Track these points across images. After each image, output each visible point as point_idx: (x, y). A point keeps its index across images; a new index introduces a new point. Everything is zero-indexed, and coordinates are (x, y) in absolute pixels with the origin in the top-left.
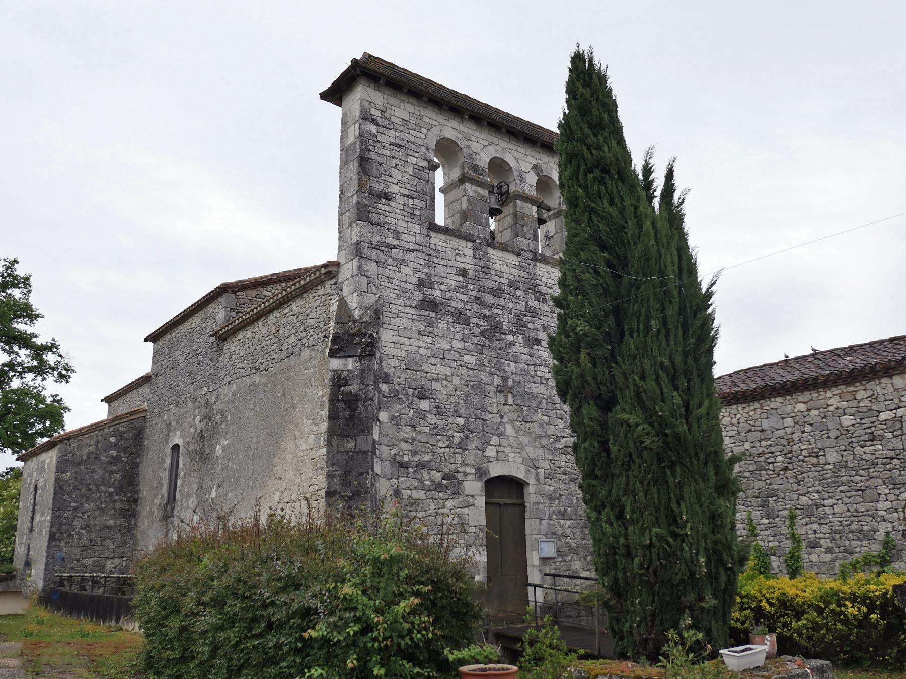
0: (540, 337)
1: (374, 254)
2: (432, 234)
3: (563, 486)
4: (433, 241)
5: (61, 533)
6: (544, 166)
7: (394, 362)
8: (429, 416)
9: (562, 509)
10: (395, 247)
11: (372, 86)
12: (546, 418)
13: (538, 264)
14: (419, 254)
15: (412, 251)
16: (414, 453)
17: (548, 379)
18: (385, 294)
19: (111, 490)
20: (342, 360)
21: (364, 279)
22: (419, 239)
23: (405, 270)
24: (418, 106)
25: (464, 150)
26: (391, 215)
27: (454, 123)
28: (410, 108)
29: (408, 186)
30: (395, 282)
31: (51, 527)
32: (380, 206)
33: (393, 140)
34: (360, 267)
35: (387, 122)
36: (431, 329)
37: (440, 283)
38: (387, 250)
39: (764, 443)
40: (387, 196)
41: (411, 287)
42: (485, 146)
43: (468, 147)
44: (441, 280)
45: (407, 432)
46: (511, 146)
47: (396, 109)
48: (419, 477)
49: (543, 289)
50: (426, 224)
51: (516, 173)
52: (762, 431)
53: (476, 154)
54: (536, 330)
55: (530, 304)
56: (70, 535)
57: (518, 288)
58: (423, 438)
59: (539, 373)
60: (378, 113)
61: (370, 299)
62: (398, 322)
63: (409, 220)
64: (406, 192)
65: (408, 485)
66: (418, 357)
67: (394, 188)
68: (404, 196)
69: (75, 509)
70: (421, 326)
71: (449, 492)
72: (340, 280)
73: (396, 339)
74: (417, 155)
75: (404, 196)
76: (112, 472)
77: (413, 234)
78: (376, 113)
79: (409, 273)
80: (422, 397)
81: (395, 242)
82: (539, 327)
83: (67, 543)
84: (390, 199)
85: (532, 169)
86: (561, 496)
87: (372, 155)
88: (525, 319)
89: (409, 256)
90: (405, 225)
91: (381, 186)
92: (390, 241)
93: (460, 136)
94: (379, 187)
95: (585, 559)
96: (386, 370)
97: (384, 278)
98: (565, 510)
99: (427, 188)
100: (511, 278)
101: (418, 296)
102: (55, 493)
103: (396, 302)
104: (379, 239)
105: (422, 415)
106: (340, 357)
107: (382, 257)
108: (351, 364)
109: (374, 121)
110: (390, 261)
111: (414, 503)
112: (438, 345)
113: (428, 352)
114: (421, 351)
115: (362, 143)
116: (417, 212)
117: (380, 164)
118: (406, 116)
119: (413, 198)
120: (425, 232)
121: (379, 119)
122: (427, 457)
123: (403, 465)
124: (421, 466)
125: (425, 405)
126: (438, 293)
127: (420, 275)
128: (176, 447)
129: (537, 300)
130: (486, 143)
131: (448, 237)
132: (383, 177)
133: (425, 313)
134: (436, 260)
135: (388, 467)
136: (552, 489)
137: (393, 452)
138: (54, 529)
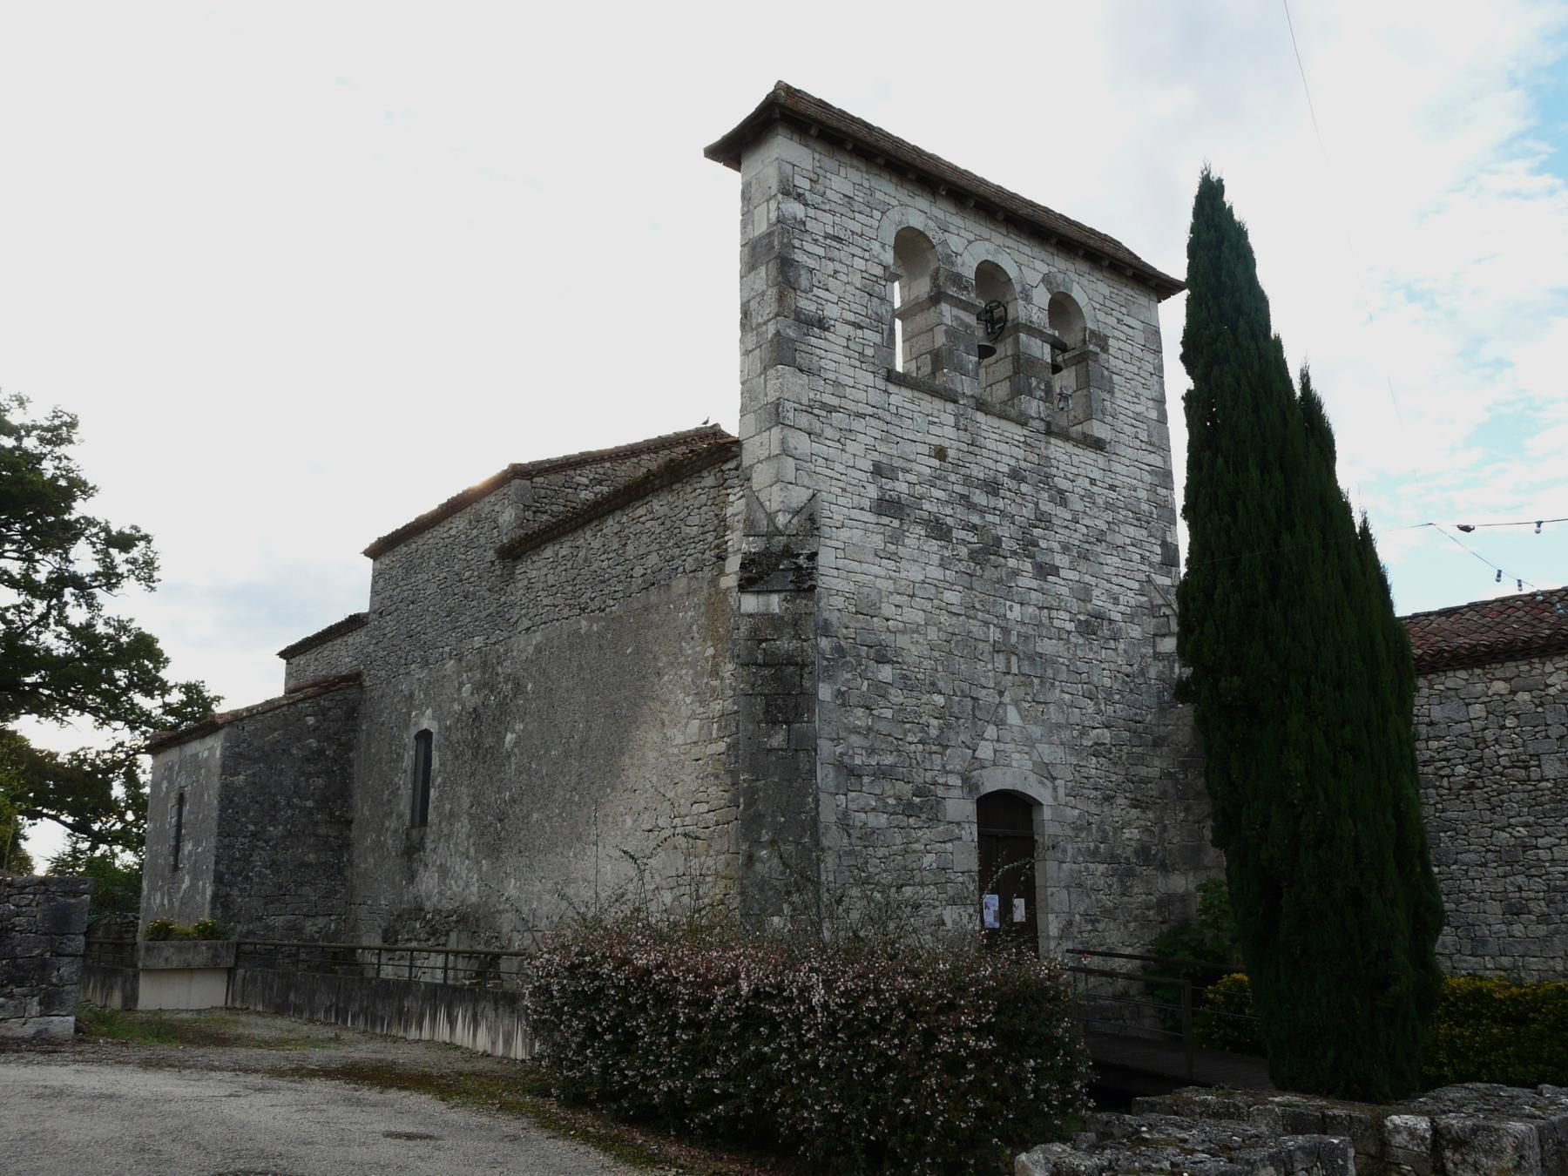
0: (1057, 563)
1: (804, 420)
2: (892, 388)
3: (1093, 809)
4: (894, 399)
5: (233, 874)
7: (839, 602)
8: (892, 691)
9: (1092, 845)
11: (796, 138)
12: (1067, 697)
13: (1053, 440)
14: (873, 422)
15: (862, 416)
16: (872, 751)
17: (1069, 632)
19: (310, 804)
20: (762, 598)
21: (791, 462)
22: (875, 397)
25: (939, 248)
26: (830, 355)
27: (922, 203)
28: (855, 176)
31: (217, 863)
34: (783, 441)
35: (819, 199)
38: (824, 413)
39: (1434, 744)
40: (822, 324)
41: (863, 476)
42: (970, 242)
43: (945, 243)
44: (908, 465)
45: (860, 718)
46: (1009, 242)
48: (878, 792)
49: (1063, 484)
50: (883, 372)
51: (1018, 288)
52: (1431, 724)
56: (247, 878)
57: (1023, 480)
58: (883, 727)
59: (1056, 623)
60: (806, 184)
61: (799, 496)
62: (844, 534)
63: (858, 364)
64: (851, 317)
65: (862, 804)
66: (874, 597)
67: (832, 311)
69: (254, 834)
70: (877, 540)
71: (924, 817)
72: (746, 463)
73: (840, 563)
74: (867, 255)
76: (309, 776)
77: (863, 387)
78: (804, 184)
79: (858, 454)
80: (882, 660)
81: (835, 401)
82: (1056, 546)
83: (241, 890)
84: (827, 329)
85: (1043, 280)
86: (1090, 824)
87: (799, 256)
88: (1036, 532)
89: (858, 425)
90: (851, 372)
91: (813, 308)
93: (932, 224)
94: (807, 305)
95: (1126, 927)
96: (826, 615)
98: (1097, 848)
100: (1013, 462)
101: (873, 492)
102: (222, 810)
103: (841, 501)
104: (812, 395)
105: (881, 689)
106: (758, 593)
107: (817, 426)
108: (775, 603)
109: (799, 197)
110: (829, 432)
111: (868, 835)
112: (904, 575)
113: (890, 585)
114: (880, 583)
116: (869, 352)
117: (811, 270)
119: (861, 328)
120: (881, 383)
122: (889, 760)
123: (854, 773)
124: (882, 773)
125: (886, 673)
126: (902, 487)
128: (424, 736)
130: (972, 237)
131: (917, 394)
134: (898, 431)
135: (832, 775)
136: (1076, 812)
137: (839, 750)
138: (222, 868)
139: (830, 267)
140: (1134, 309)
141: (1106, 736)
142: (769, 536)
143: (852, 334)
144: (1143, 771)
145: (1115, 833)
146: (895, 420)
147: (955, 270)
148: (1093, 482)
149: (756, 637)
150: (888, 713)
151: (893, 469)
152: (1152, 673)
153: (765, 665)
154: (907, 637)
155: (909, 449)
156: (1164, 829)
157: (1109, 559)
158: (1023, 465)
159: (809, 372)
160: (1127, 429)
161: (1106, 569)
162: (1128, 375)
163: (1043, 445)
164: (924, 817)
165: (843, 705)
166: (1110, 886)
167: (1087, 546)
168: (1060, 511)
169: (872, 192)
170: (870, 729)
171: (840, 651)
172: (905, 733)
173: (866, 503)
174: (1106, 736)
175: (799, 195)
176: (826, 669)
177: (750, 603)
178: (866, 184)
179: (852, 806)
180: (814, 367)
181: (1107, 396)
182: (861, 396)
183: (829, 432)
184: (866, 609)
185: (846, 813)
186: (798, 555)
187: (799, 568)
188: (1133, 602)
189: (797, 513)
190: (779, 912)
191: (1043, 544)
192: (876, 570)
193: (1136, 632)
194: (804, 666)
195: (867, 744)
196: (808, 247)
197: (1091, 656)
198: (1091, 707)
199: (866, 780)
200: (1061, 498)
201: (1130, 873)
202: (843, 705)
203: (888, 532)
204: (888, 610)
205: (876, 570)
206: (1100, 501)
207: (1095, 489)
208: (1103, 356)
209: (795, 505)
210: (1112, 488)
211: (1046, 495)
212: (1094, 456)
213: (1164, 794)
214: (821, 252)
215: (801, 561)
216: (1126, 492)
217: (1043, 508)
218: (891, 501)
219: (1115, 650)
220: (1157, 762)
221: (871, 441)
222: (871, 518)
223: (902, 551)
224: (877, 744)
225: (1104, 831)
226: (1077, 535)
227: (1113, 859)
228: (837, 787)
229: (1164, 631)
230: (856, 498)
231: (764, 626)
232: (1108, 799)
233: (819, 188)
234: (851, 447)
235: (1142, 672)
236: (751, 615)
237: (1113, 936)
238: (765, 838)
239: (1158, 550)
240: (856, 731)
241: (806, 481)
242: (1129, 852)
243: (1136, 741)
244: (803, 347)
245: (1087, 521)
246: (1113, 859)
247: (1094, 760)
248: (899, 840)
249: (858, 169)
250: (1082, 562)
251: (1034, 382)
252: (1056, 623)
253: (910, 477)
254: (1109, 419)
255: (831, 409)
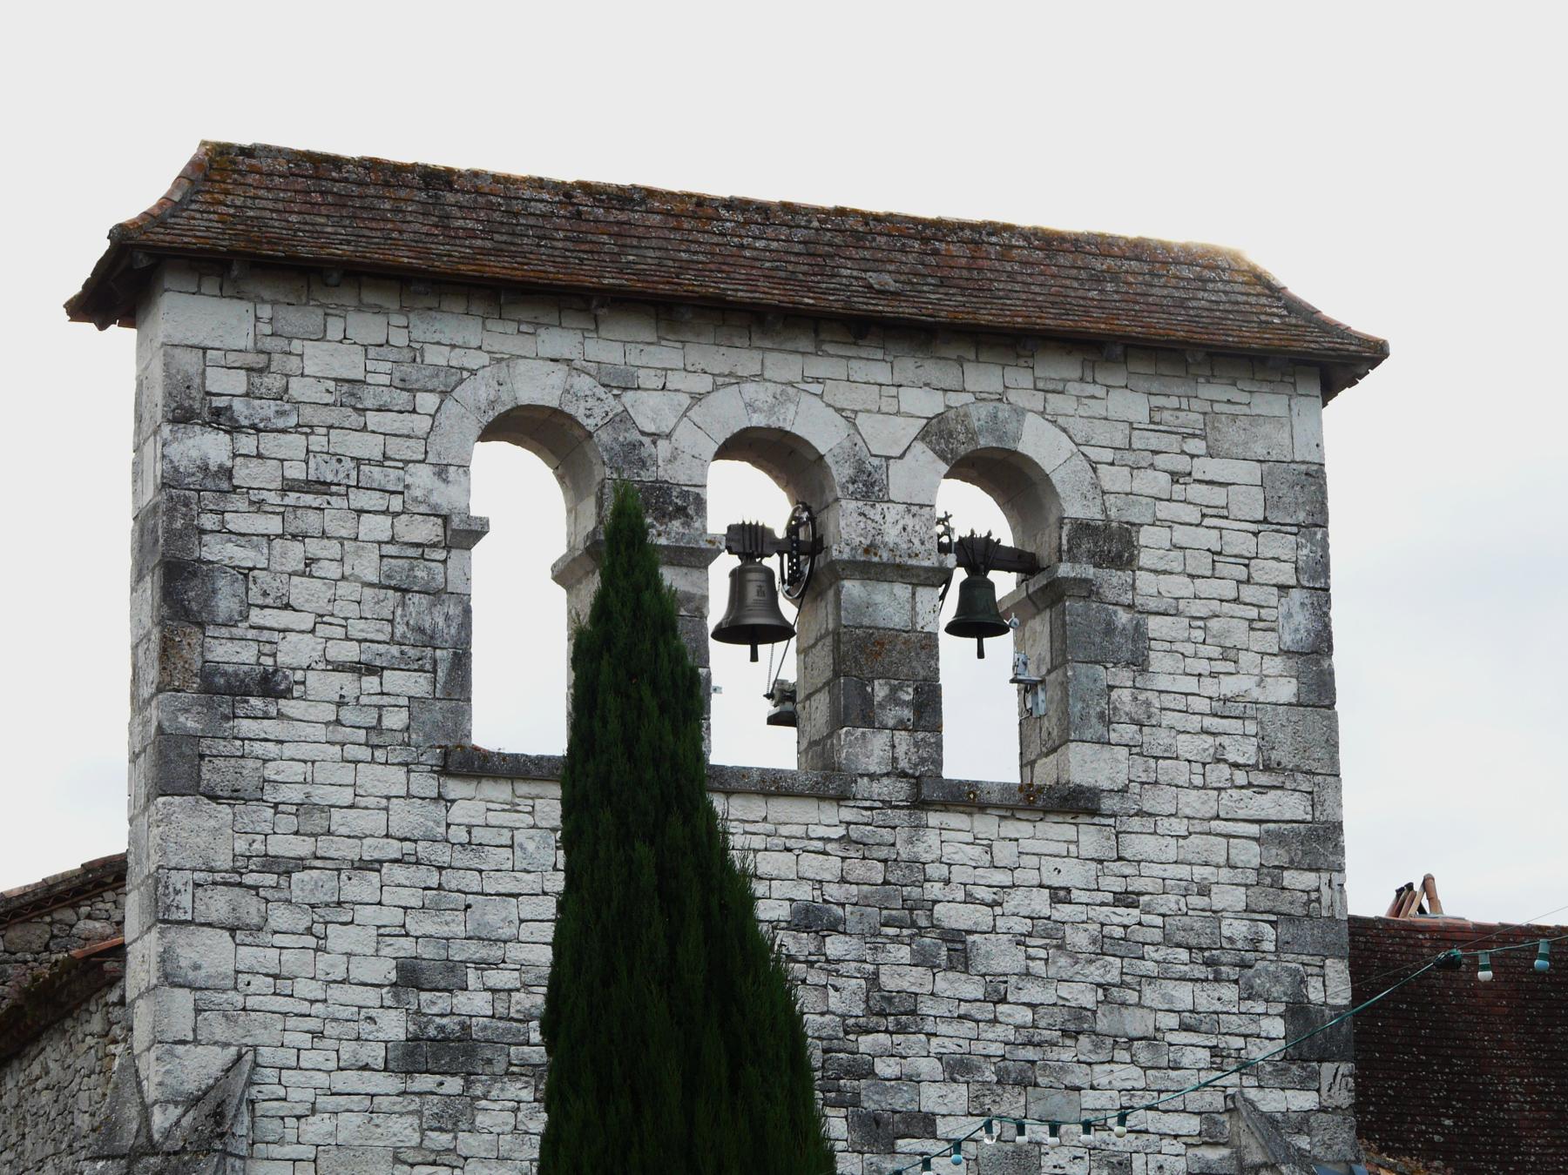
1: (218, 904)
2: (454, 788)
4: (458, 813)
6: (979, 415)
10: (301, 864)
11: (210, 285)
13: (934, 818)
14: (399, 873)
15: (374, 865)
18: (261, 1036)
21: (183, 1000)
22: (406, 817)
23: (340, 939)
24: (403, 310)
25: (604, 437)
26: (289, 750)
27: (560, 341)
28: (367, 327)
29: (357, 628)
30: (304, 988)
32: (246, 727)
33: (296, 472)
34: (165, 957)
35: (269, 408)
36: (444, 1139)
37: (483, 965)
38: (270, 879)
40: (270, 685)
41: (371, 997)
42: (697, 398)
43: (624, 418)
44: (495, 953)
46: (820, 367)
47: (310, 348)
49: (953, 915)
50: (432, 758)
51: (840, 473)
53: (655, 437)
54: (914, 1080)
55: (889, 982)
57: (835, 926)
60: (236, 382)
61: (201, 1066)
62: (316, 1128)
63: (364, 753)
64: (349, 652)
67: (295, 651)
68: (339, 667)
70: (403, 1130)
72: (130, 996)
74: (396, 503)
75: (339, 667)
77: (381, 799)
78: (227, 383)
81: (302, 847)
82: (928, 1067)
84: (286, 694)
85: (924, 435)
87: (215, 550)
88: (866, 1043)
89: (360, 888)
90: (346, 774)
91: (248, 654)
92: (287, 846)
93: (584, 384)
97: (259, 983)
99: (436, 619)
100: (804, 893)
101: (394, 1026)
103: (308, 1059)
104: (241, 845)
107: (251, 908)
109: (221, 419)
110: (281, 917)
115: (171, 512)
116: (395, 719)
117: (246, 573)
118: (349, 363)
119: (372, 670)
120: (425, 784)
121: (239, 406)
126: (474, 1003)
127: (406, 947)
129: (923, 960)
130: (702, 384)
131: (523, 788)
132: (256, 616)
133: (425, 1082)
134: (472, 881)
139: (296, 551)
140: (1231, 435)
146: (462, 858)
147: (647, 476)
148: (1060, 895)
151: (450, 967)
155: (496, 916)
157: (1101, 1074)
158: (834, 892)
159: (236, 796)
160: (1188, 746)
161: (1089, 1099)
162: (1199, 609)
163: (902, 834)
167: (1030, 1053)
168: (946, 983)
169: (415, 353)
173: (375, 1054)
175: (217, 412)
178: (399, 338)
180: (248, 783)
181: (1123, 676)
182: (373, 821)
183: (281, 917)
189: (194, 1101)
191: (885, 1068)
196: (235, 522)
200: (957, 950)
203: (433, 1105)
206: (1079, 939)
207: (1064, 912)
208: (1112, 580)
209: (191, 1087)
210: (1125, 899)
211: (904, 953)
212: (1068, 831)
214: (273, 525)
216: (1170, 903)
217: (889, 982)
218: (443, 1040)
221: (392, 916)
222: (391, 1083)
223: (468, 1143)
230: (347, 1049)
233: (273, 382)
234: (340, 939)
239: (1277, 1027)
241: (220, 1030)
244: (221, 746)
245: (1033, 993)
249: (379, 310)
251: (880, 690)
253: (496, 978)
254: (1127, 732)
255: (285, 867)
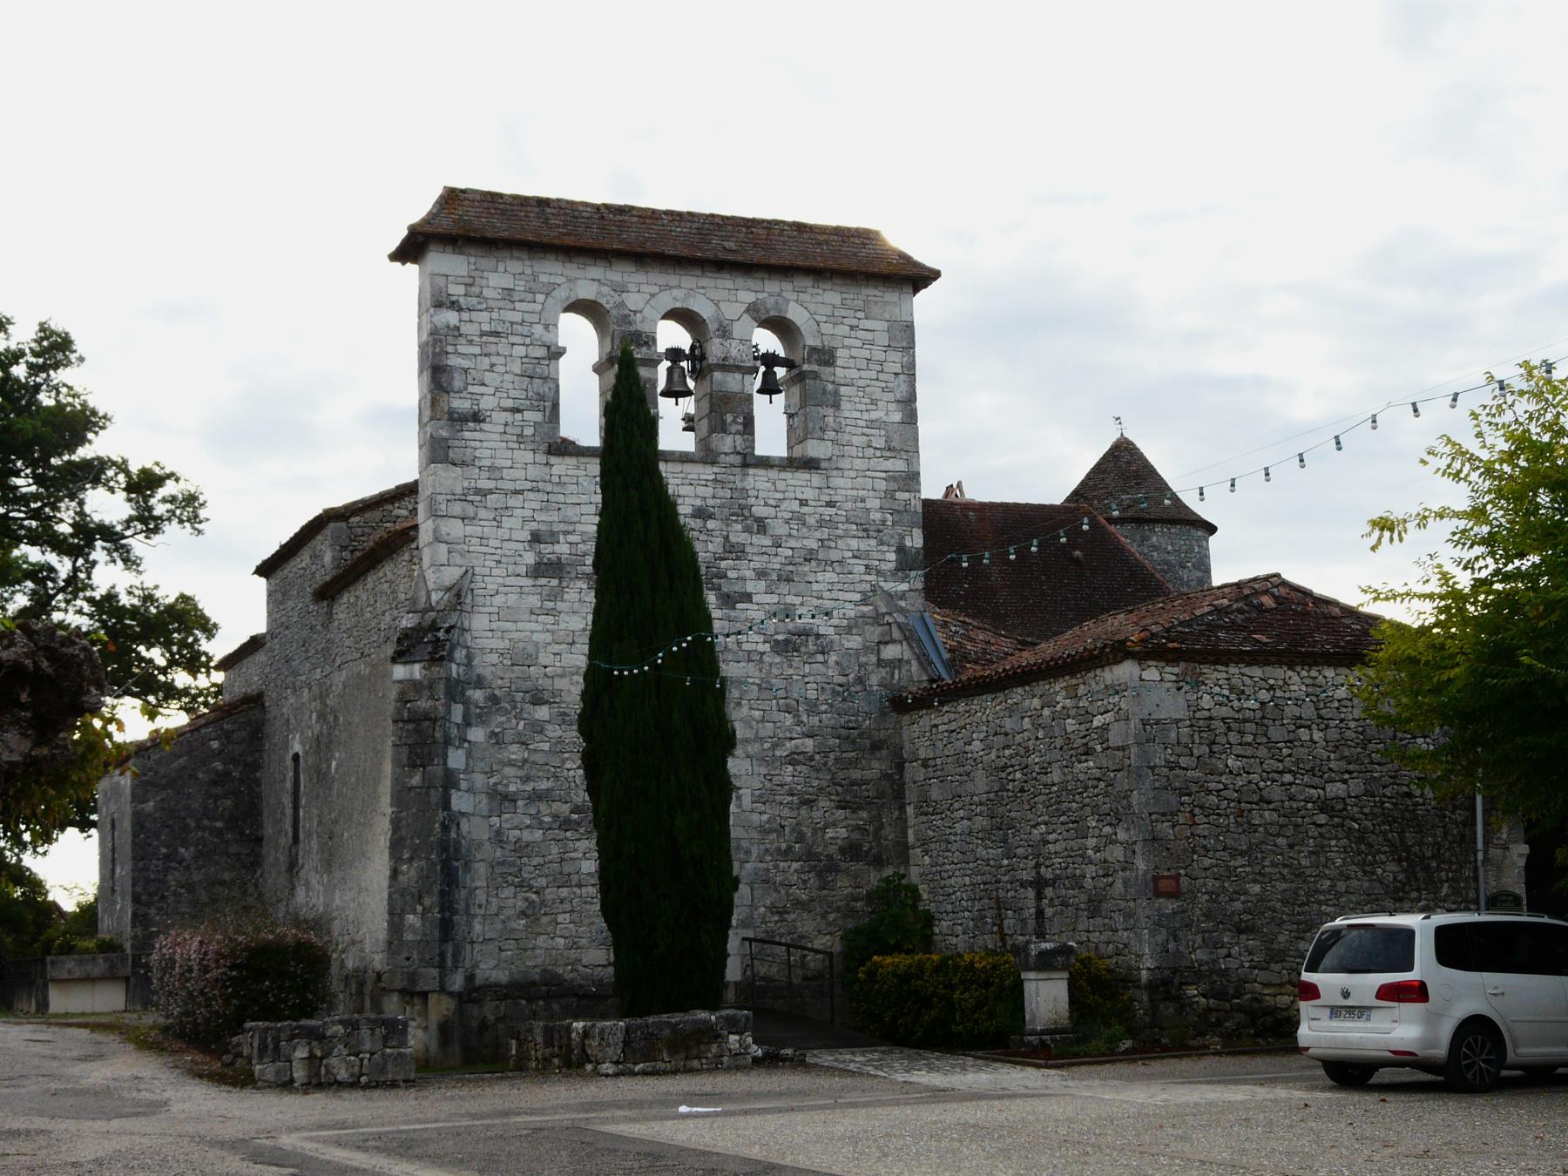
1: (457, 508)
2: (553, 460)
3: (786, 812)
4: (555, 470)
5: (150, 895)
6: (771, 302)
7: (494, 658)
8: (549, 727)
9: (784, 846)
10: (491, 492)
11: (449, 249)
12: (757, 714)
13: (751, 471)
14: (531, 495)
16: (526, 779)
17: (762, 654)
18: (475, 562)
19: (219, 824)
20: (408, 667)
21: (443, 548)
22: (533, 472)
23: (506, 522)
24: (530, 259)
25: (614, 312)
26: (485, 444)
27: (596, 271)
28: (515, 266)
29: (512, 393)
30: (493, 543)
31: (134, 885)
32: (467, 435)
33: (486, 328)
34: (435, 531)
35: (475, 301)
36: (551, 604)
37: (566, 533)
39: (1007, 752)
40: (477, 417)
41: (520, 546)
42: (653, 295)
43: (622, 304)
44: (571, 528)
45: (515, 752)
46: (705, 282)
47: (491, 275)
48: (533, 811)
49: (759, 511)
50: (544, 447)
51: (712, 327)
52: (1006, 734)
53: (635, 312)
54: (743, 579)
55: (733, 539)
56: (163, 898)
57: (711, 516)
58: (539, 758)
59: (745, 646)
60: (461, 290)
61: (451, 575)
63: (516, 445)
64: (509, 403)
65: (516, 823)
66: (531, 649)
67: (487, 403)
68: (505, 410)
69: (167, 857)
70: (534, 601)
71: (582, 830)
73: (494, 626)
74: (528, 341)
75: (505, 410)
76: (217, 798)
77: (523, 464)
78: (456, 290)
79: (516, 528)
80: (538, 701)
81: (491, 485)
82: (749, 574)
83: (159, 909)
84: (484, 421)
85: (747, 311)
86: (783, 827)
87: (453, 361)
88: (723, 564)
89: (512, 502)
90: (509, 454)
91: (467, 404)
92: (485, 484)
93: (605, 290)
94: (461, 404)
95: (824, 917)
96: (479, 671)
97: (475, 541)
98: (789, 848)
99: (545, 389)
100: (698, 502)
101: (530, 558)
102: (135, 835)
104: (466, 484)
105: (538, 728)
106: (405, 663)
107: (470, 510)
108: (417, 671)
109: (454, 306)
110: (482, 513)
111: (521, 848)
112: (563, 626)
113: (548, 637)
114: (535, 637)
115: (434, 345)
116: (529, 431)
117: (466, 371)
118: (507, 282)
119: (519, 411)
120: (541, 458)
121: (461, 300)
122: (544, 785)
123: (510, 799)
124: (537, 797)
125: (543, 713)
126: (562, 549)
127: (534, 526)
128: (296, 757)
129: (747, 530)
130: (655, 289)
131: (582, 460)
132: (470, 389)
133: (543, 581)
134: (561, 498)
135: (485, 801)
136: (765, 817)
137: (492, 781)
138: (139, 889)
139: (487, 361)
140: (876, 309)
141: (809, 744)
142: (424, 612)
143: (510, 420)
144: (856, 774)
145: (815, 831)
146: (557, 489)
147: (632, 329)
148: (804, 503)
149: (403, 699)
150: (546, 747)
151: (553, 534)
152: (874, 680)
153: (409, 721)
154: (566, 680)
155: (571, 513)
156: (882, 826)
157: (820, 577)
158: (710, 502)
159: (463, 464)
160: (856, 440)
161: (815, 587)
162: (861, 383)
163: (738, 478)
164: (582, 830)
165: (497, 743)
166: (805, 882)
167: (791, 568)
168: (756, 539)
169: (535, 278)
170: (525, 761)
171: (494, 699)
172: (563, 761)
173: (523, 570)
174: (809, 744)
175: (453, 303)
176: (479, 716)
177: (400, 672)
178: (528, 271)
179: (505, 825)
180: (468, 458)
181: (830, 411)
182: (520, 474)
183: (482, 513)
184: (522, 658)
185: (499, 832)
186: (438, 630)
187: (438, 640)
188: (852, 614)
189: (448, 589)
190: (414, 912)
191: (731, 574)
192: (533, 626)
193: (854, 642)
194: (436, 720)
195: (521, 773)
196: (461, 349)
197: (791, 672)
198: (789, 720)
199: (520, 803)
200: (761, 526)
201: (832, 868)
202: (497, 743)
203: (546, 591)
204: (544, 659)
205: (533, 626)
206: (811, 521)
207: (805, 509)
208: (826, 371)
209: (447, 583)
210: (830, 504)
211: (739, 527)
212: (807, 476)
213: (880, 795)
214: (477, 350)
215: (441, 634)
216: (849, 505)
217: (733, 539)
218: (550, 564)
219: (825, 663)
220: (875, 764)
221: (528, 513)
222: (529, 582)
223: (560, 606)
224: (533, 772)
225: (800, 832)
226: (778, 559)
227: (810, 856)
228: (491, 810)
229: (887, 638)
230: (511, 568)
231: (410, 689)
232: (809, 803)
233: (476, 290)
234: (506, 522)
235: (860, 680)
236: (400, 682)
237: (806, 924)
238: (406, 856)
239: (893, 557)
240: (511, 763)
241: (459, 560)
242: (832, 849)
243: (846, 746)
244: (457, 443)
245: (793, 543)
246: (810, 856)
247: (790, 768)
248: (555, 850)
249: (519, 259)
250: (783, 584)
251: (729, 418)
252: (745, 646)
253: (571, 538)
254: (832, 434)
255: (484, 493)
